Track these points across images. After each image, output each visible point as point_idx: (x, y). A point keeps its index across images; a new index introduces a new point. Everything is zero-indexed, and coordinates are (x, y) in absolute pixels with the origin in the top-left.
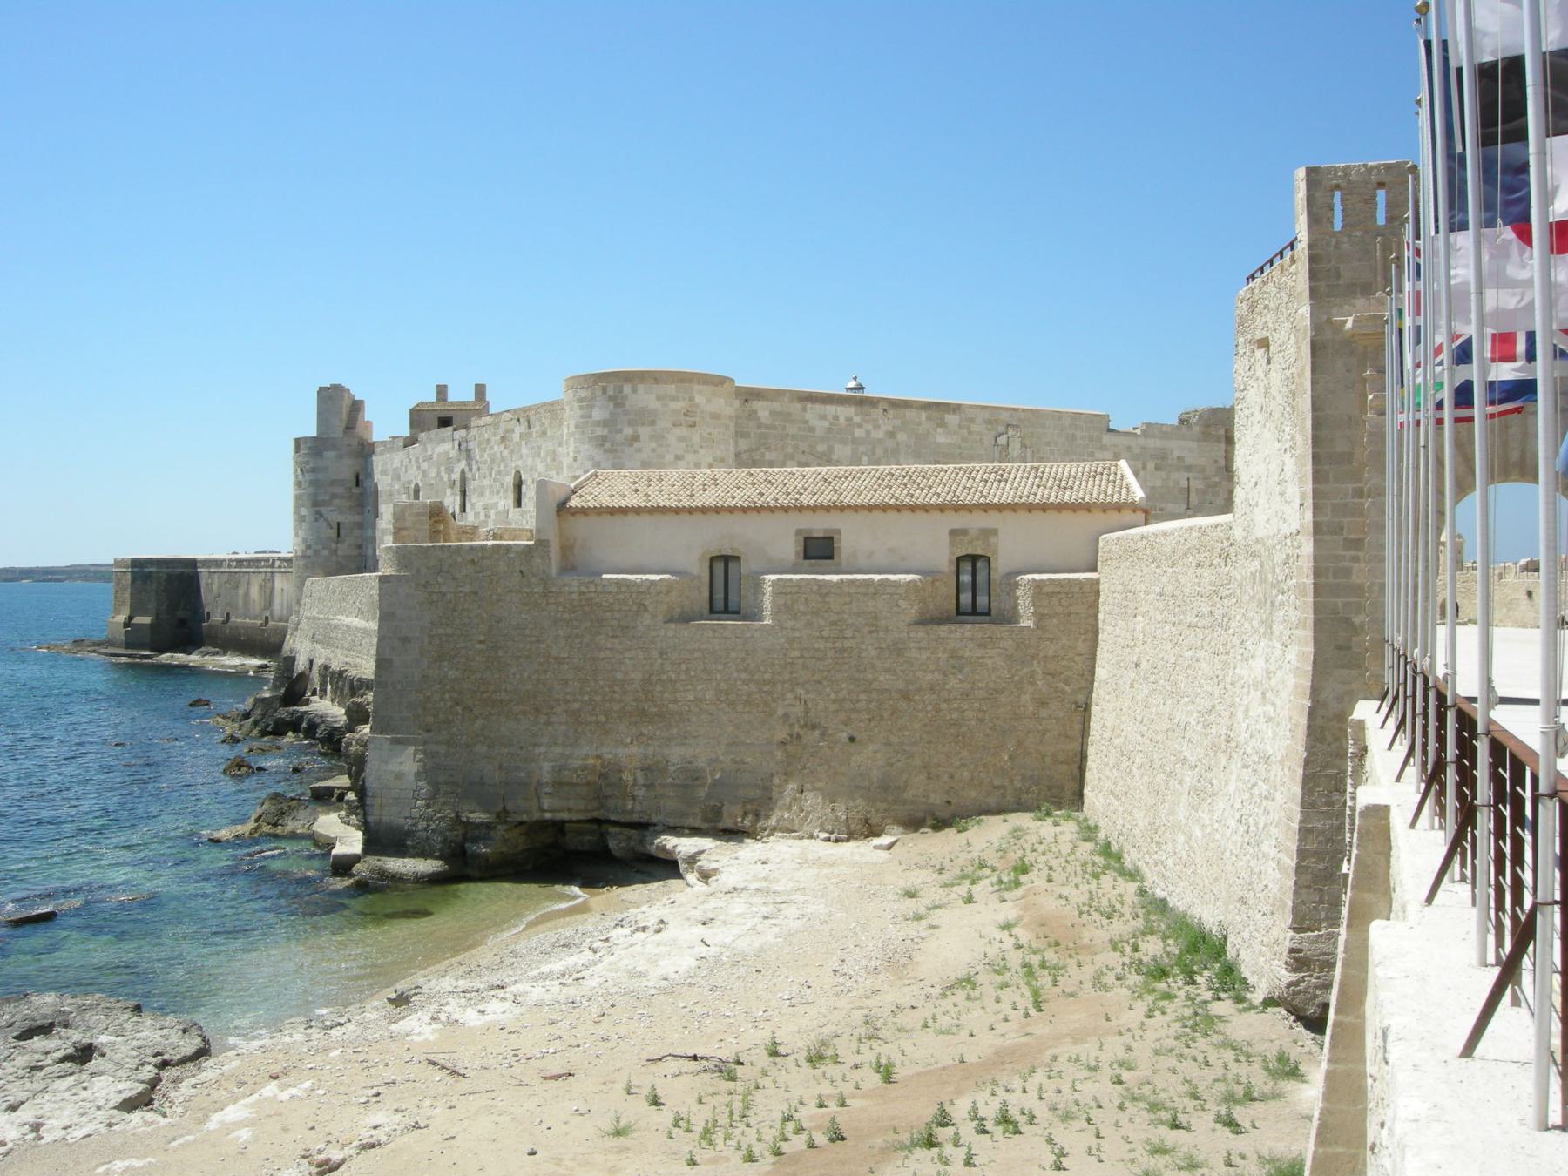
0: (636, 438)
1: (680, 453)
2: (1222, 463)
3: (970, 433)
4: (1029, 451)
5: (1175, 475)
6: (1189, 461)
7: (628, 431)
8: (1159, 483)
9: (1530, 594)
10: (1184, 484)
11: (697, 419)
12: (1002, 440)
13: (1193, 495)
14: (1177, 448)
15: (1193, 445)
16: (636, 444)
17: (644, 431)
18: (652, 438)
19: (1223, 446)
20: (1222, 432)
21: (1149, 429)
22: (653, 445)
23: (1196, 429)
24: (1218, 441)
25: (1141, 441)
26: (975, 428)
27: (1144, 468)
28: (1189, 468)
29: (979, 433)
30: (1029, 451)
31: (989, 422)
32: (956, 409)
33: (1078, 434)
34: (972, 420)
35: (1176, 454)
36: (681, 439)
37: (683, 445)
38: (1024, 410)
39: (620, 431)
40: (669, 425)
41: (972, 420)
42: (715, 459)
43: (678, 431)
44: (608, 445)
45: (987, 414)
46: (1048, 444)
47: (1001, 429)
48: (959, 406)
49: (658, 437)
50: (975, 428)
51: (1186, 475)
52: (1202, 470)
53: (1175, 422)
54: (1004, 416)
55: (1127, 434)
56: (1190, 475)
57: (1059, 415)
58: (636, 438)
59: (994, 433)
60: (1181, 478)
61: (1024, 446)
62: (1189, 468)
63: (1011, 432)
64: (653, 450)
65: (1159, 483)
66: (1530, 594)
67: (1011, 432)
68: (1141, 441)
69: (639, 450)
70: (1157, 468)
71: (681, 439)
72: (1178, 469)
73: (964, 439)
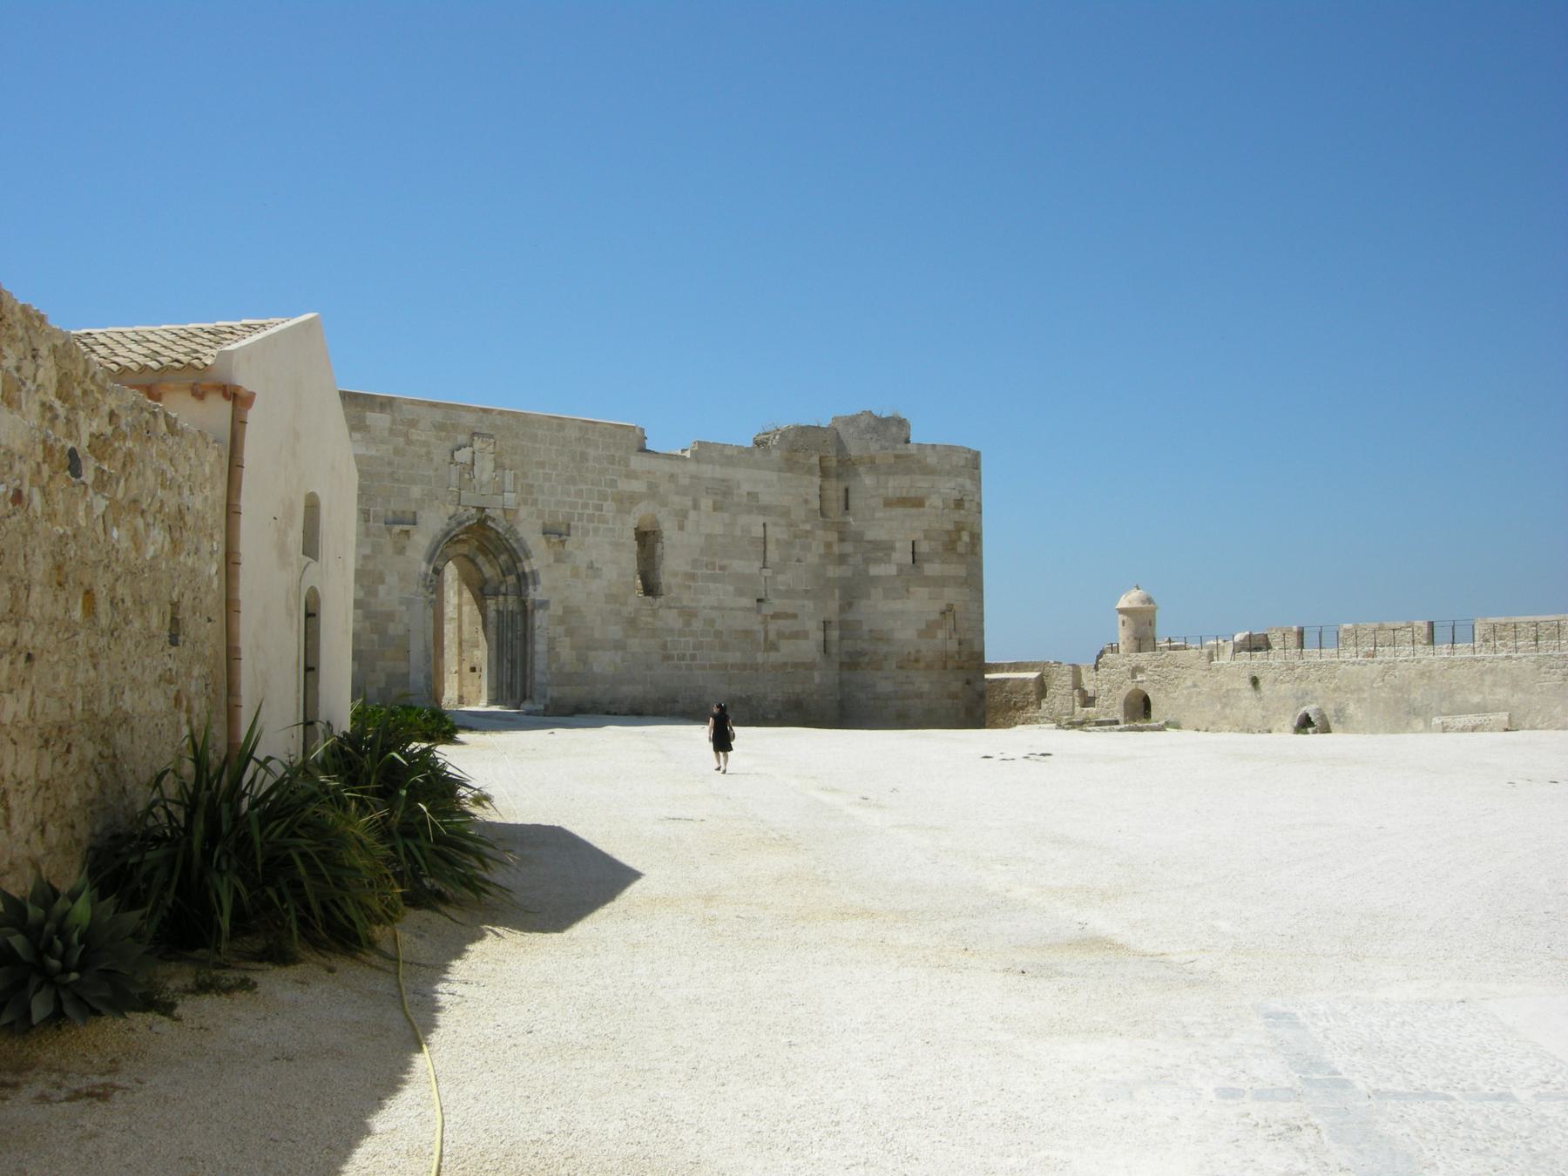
2: (816, 504)
3: (409, 442)
4: (509, 475)
5: (743, 519)
6: (765, 499)
8: (718, 529)
9: (1255, 682)
10: (758, 532)
12: (463, 456)
13: (771, 547)
14: (746, 480)
15: (772, 476)
19: (817, 480)
20: (815, 460)
21: (704, 451)
23: (776, 454)
24: (810, 471)
25: (692, 468)
26: (415, 435)
27: (696, 506)
28: (764, 510)
29: (426, 444)
30: (509, 475)
31: (441, 427)
32: (386, 404)
33: (591, 452)
34: (413, 423)
35: (746, 488)
38: (501, 413)
41: (413, 423)
45: (438, 416)
46: (541, 465)
47: (462, 438)
48: (391, 401)
50: (415, 435)
51: (761, 519)
52: (786, 513)
53: (750, 444)
54: (469, 420)
55: (670, 457)
56: (767, 519)
57: (561, 423)
59: (449, 445)
60: (755, 524)
61: (499, 466)
62: (764, 510)
63: (478, 444)
66: (1255, 682)
67: (478, 444)
68: (692, 468)
70: (717, 508)
72: (749, 511)
73: (396, 451)
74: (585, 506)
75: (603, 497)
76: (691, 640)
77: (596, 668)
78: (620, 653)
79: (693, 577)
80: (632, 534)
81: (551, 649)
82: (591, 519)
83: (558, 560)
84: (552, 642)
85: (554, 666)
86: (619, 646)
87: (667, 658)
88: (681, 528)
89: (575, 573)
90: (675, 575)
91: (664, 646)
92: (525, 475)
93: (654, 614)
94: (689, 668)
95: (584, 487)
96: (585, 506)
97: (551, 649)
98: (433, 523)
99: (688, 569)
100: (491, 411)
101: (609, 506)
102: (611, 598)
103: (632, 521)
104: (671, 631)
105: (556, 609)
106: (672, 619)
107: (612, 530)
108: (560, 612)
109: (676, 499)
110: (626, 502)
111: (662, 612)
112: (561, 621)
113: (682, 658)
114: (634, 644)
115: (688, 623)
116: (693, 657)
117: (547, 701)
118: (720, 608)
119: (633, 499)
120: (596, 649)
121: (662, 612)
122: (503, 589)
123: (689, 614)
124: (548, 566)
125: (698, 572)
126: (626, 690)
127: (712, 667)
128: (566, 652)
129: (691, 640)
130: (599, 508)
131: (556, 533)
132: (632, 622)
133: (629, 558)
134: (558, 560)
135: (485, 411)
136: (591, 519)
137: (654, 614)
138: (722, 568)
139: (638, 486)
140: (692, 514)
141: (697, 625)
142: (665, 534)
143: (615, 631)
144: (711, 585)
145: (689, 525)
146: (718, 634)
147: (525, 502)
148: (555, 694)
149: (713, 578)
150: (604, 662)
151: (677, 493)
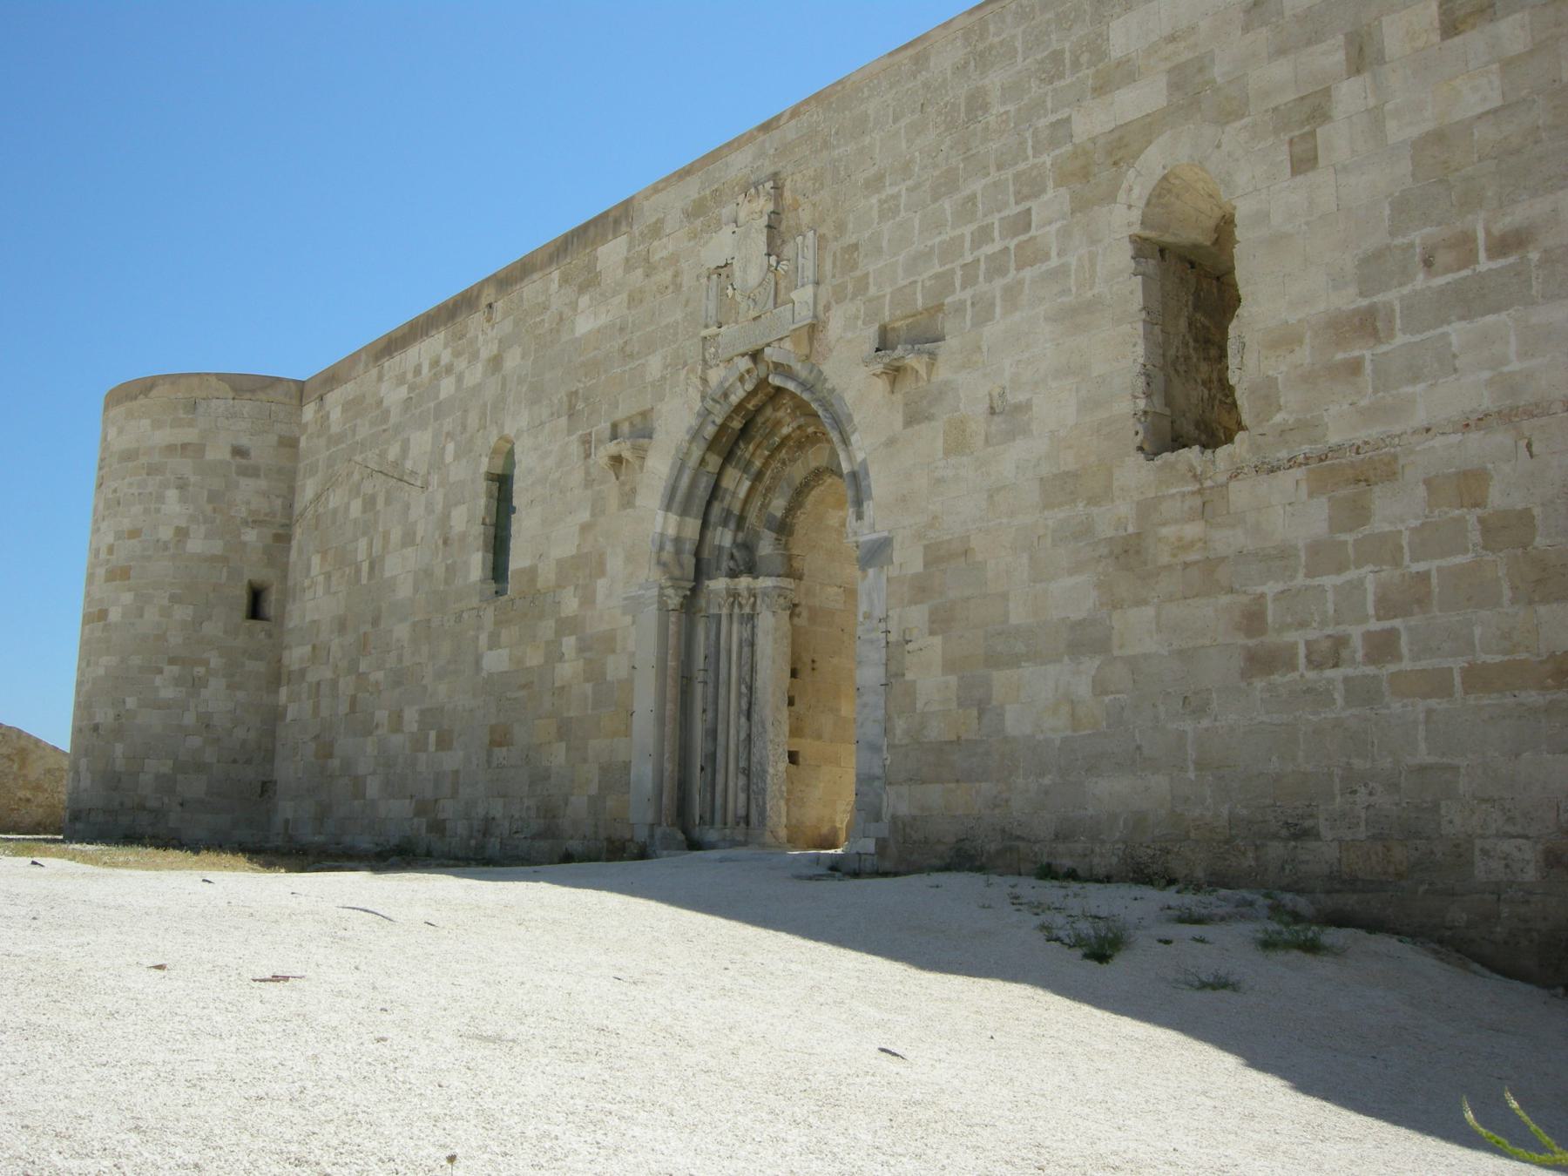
38: (795, 112)
42: (119, 535)
45: (692, 189)
48: (627, 205)
65: (1476, 93)
74: (983, 235)
75: (1031, 187)
76: (1370, 578)
77: (1016, 722)
78: (1091, 665)
79: (1367, 324)
80: (1122, 256)
81: (893, 677)
82: (997, 267)
83: (913, 417)
84: (895, 650)
85: (900, 725)
86: (1085, 640)
87: (1262, 662)
88: (1303, 163)
89: (957, 443)
90: (1285, 340)
91: (1253, 620)
92: (841, 227)
93: (1208, 506)
94: (1363, 693)
95: (977, 186)
96: (983, 235)
97: (893, 677)
98: (679, 419)
99: (1348, 300)
100: (778, 118)
101: (1051, 205)
102: (1061, 487)
103: (1122, 219)
104: (1284, 554)
105: (908, 559)
106: (1286, 511)
107: (1061, 272)
108: (917, 566)
109: (1281, 70)
110: (1092, 172)
111: (1241, 494)
112: (920, 589)
113: (1335, 653)
114: (1139, 631)
115: (1358, 513)
116: (1382, 647)
117: (883, 829)
118: (1513, 414)
119: (1121, 147)
120: (1015, 661)
121: (1241, 494)
123: (1353, 476)
124: (891, 442)
125: (1392, 297)
126: (1112, 792)
127: (1477, 678)
128: (931, 682)
129: (1370, 578)
130: (1023, 223)
131: (901, 345)
132: (1129, 552)
133: (1116, 351)
134: (913, 417)
135: (766, 127)
136: (997, 267)
137: (1208, 506)
138: (1503, 245)
139: (1140, 99)
140: (1350, 95)
141: (1395, 511)
142: (1243, 210)
143: (1072, 594)
144: (1457, 332)
145: (1337, 139)
146: (1509, 530)
147: (839, 296)
148: (904, 809)
149: (1468, 301)
150: (1040, 701)
151: (1281, 52)
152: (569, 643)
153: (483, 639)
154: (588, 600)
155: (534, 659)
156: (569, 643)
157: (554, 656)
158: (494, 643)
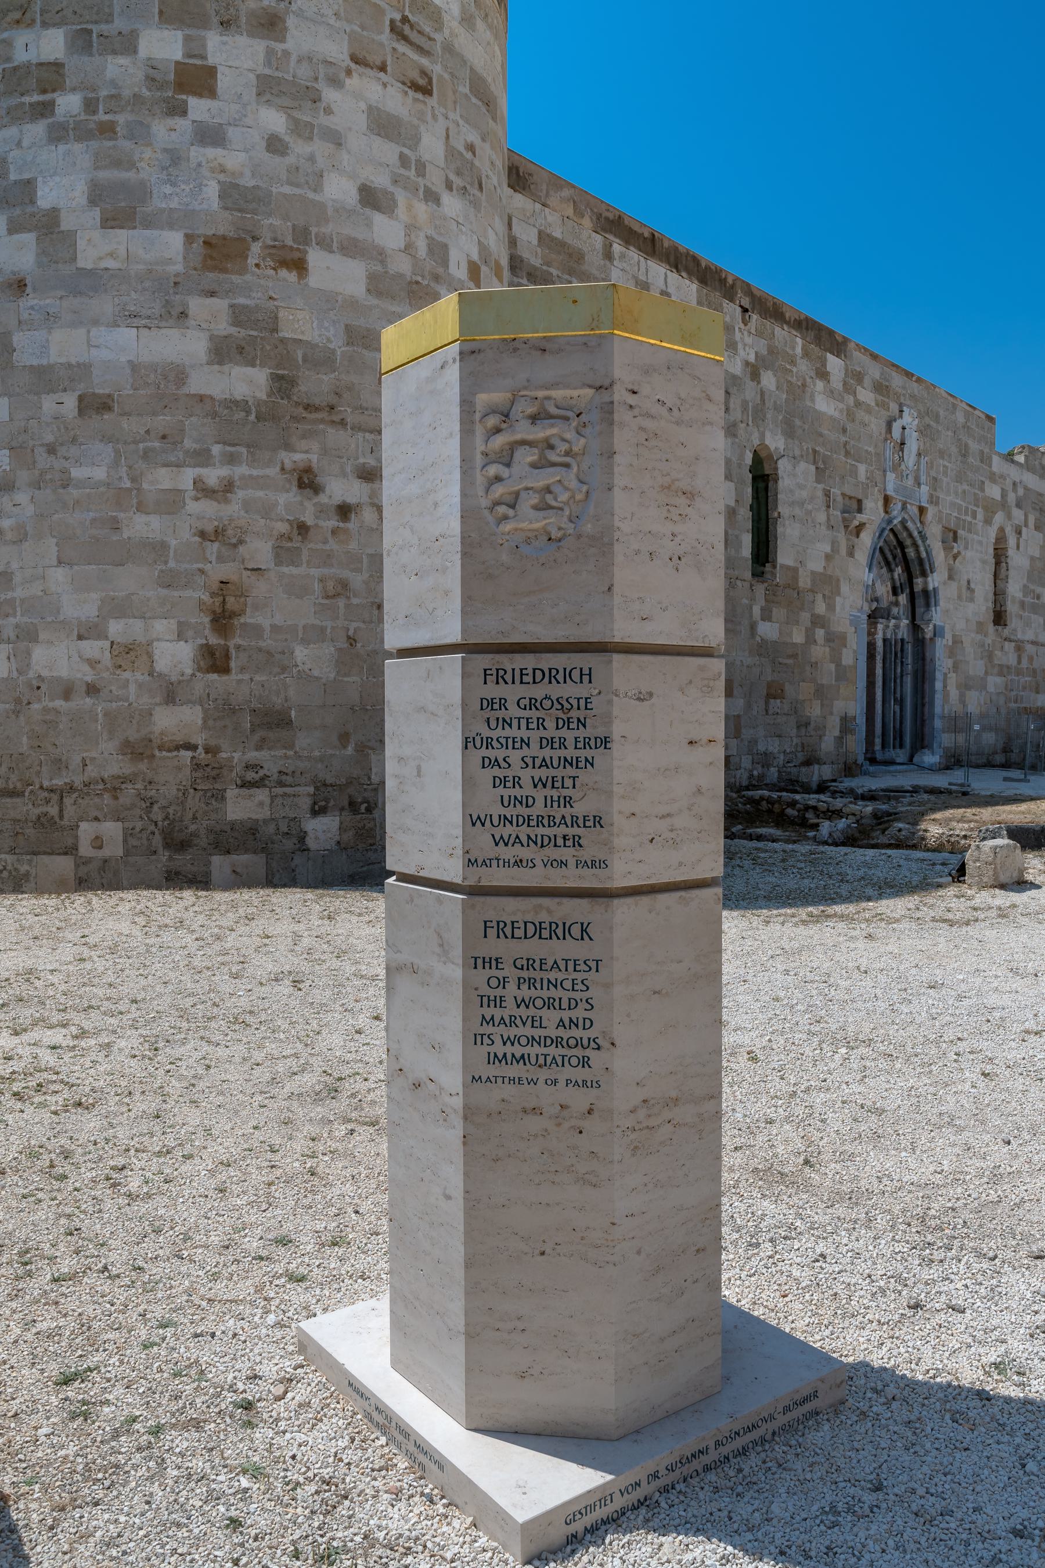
0: (196, 79)
1: (381, 180)
7: (163, 45)
11: (437, 70)
16: (198, 107)
17: (236, 57)
18: (267, 88)
22: (273, 120)
36: (383, 125)
37: (388, 151)
39: (128, 44)
40: (338, 51)
43: (370, 90)
44: (69, 103)
49: (293, 92)
58: (196, 79)
64: (275, 145)
69: (210, 135)
71: (383, 125)
122: (895, 610)
152: (820, 633)
153: (756, 610)
154: (831, 607)
155: (798, 637)
156: (820, 633)
157: (810, 640)
158: (766, 616)
